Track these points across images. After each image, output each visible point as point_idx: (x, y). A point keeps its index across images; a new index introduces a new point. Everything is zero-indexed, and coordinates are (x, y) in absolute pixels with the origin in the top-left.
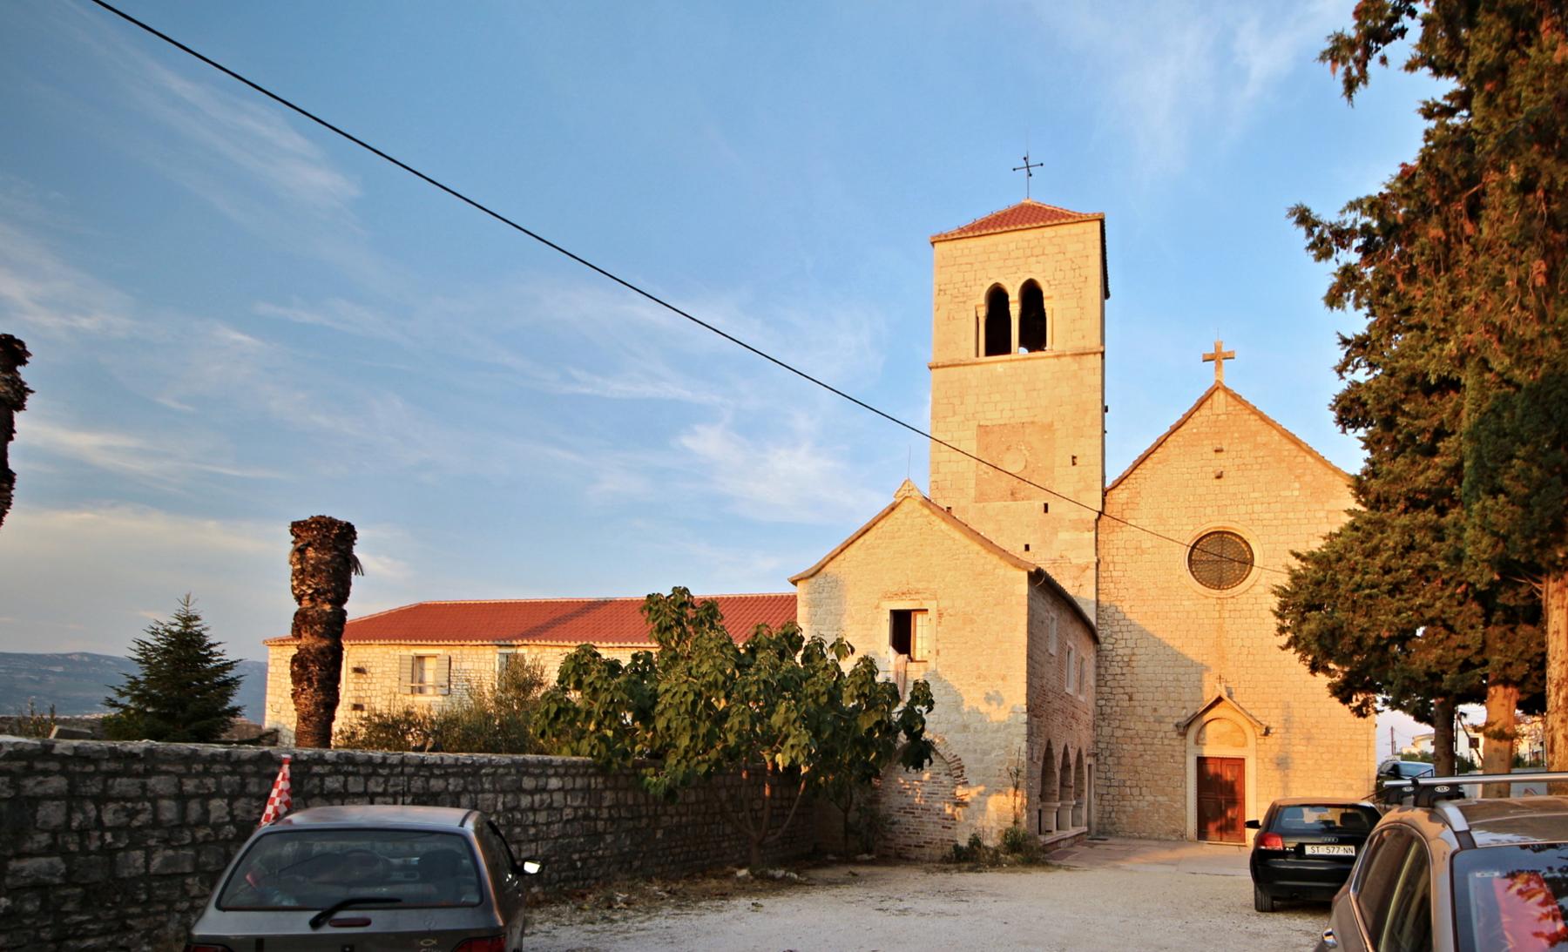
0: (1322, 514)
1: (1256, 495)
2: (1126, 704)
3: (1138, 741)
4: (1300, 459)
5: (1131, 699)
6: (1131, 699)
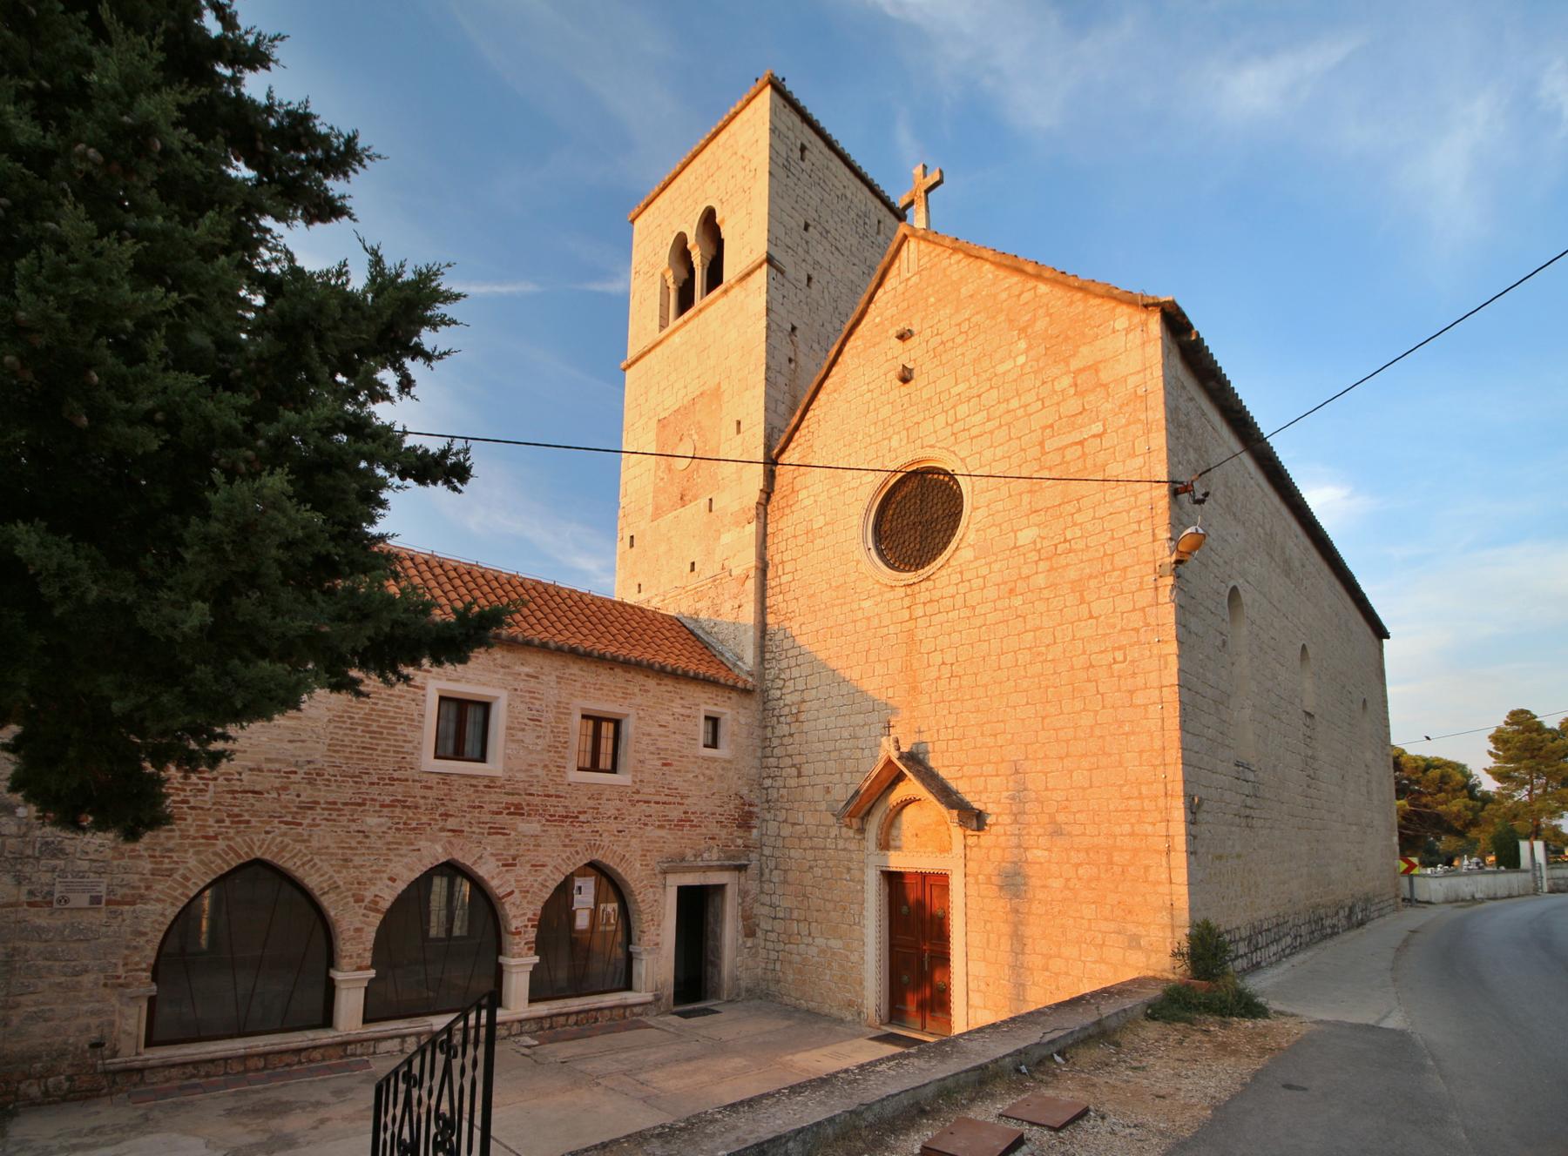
0: (1066, 381)
1: (962, 387)
2: (792, 782)
4: (1026, 297)
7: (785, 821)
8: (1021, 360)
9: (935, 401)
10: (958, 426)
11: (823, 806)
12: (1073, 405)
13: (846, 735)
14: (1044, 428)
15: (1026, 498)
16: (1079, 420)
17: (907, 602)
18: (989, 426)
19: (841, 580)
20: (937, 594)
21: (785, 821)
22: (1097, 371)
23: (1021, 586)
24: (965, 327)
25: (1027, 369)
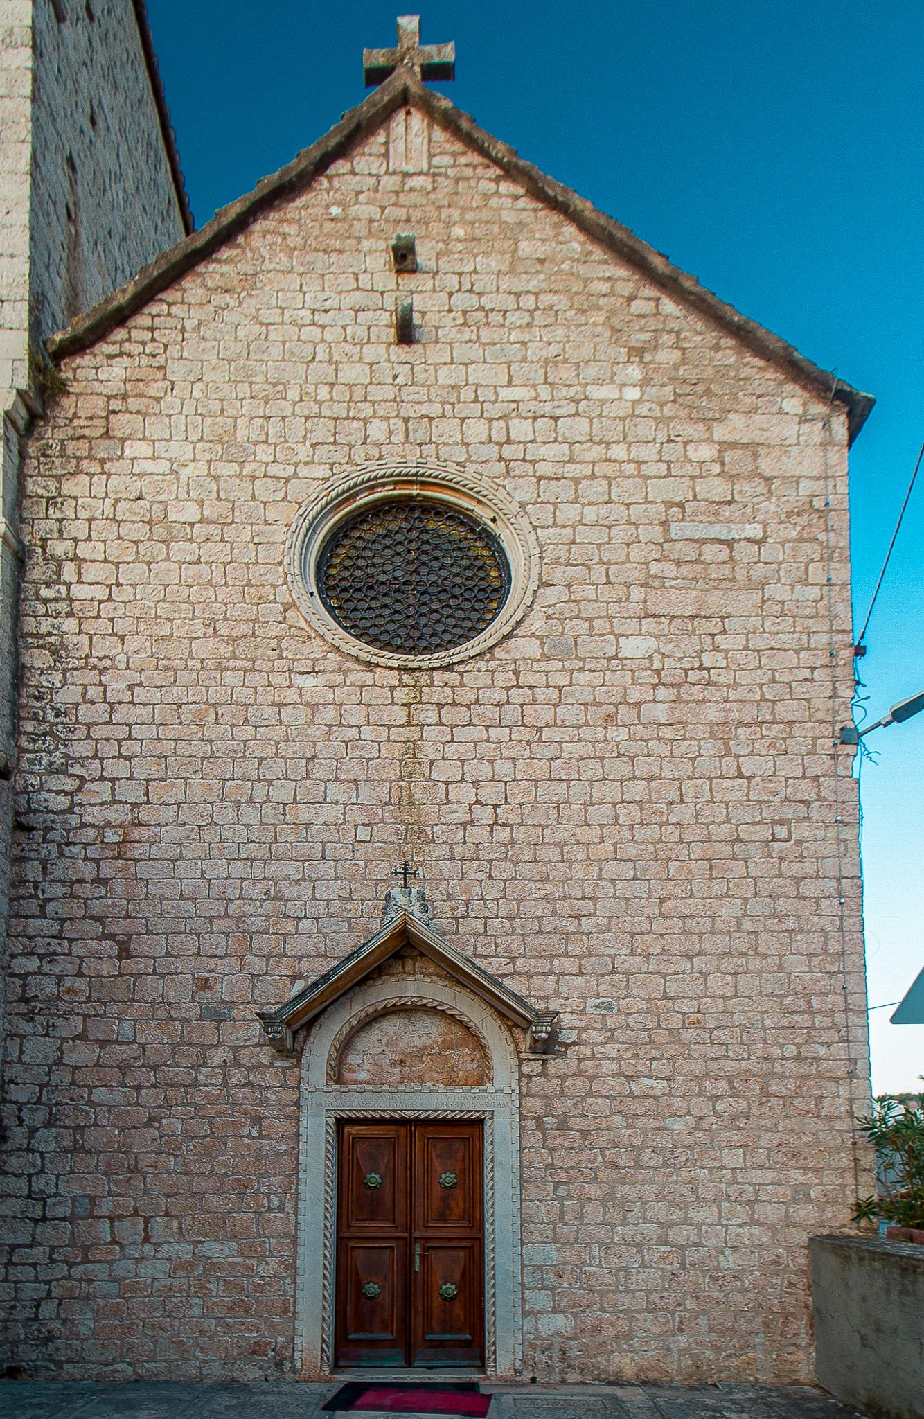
0: (706, 452)
1: (518, 393)
3: (142, 1075)
4: (638, 306)
5: (125, 952)
6: (125, 952)
7: (83, 1036)
8: (632, 394)
9: (467, 394)
10: (508, 451)
11: (193, 1012)
12: (717, 489)
13: (255, 891)
14: (669, 504)
15: (637, 594)
16: (726, 511)
17: (402, 695)
18: (571, 470)
19: (244, 629)
20: (466, 696)
21: (83, 1036)
22: (756, 456)
23: (625, 713)
24: (528, 302)
25: (643, 410)
